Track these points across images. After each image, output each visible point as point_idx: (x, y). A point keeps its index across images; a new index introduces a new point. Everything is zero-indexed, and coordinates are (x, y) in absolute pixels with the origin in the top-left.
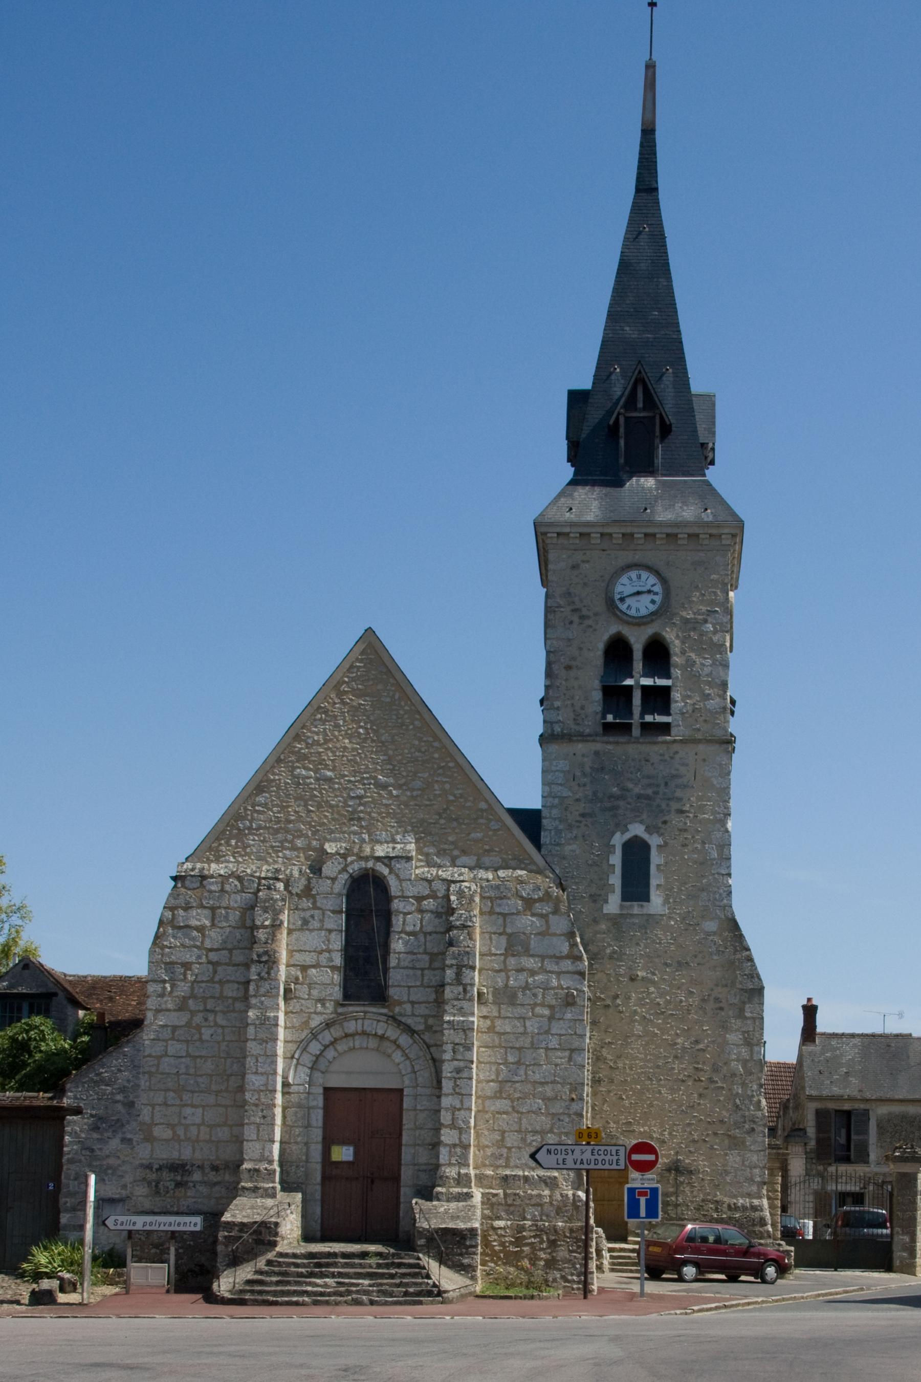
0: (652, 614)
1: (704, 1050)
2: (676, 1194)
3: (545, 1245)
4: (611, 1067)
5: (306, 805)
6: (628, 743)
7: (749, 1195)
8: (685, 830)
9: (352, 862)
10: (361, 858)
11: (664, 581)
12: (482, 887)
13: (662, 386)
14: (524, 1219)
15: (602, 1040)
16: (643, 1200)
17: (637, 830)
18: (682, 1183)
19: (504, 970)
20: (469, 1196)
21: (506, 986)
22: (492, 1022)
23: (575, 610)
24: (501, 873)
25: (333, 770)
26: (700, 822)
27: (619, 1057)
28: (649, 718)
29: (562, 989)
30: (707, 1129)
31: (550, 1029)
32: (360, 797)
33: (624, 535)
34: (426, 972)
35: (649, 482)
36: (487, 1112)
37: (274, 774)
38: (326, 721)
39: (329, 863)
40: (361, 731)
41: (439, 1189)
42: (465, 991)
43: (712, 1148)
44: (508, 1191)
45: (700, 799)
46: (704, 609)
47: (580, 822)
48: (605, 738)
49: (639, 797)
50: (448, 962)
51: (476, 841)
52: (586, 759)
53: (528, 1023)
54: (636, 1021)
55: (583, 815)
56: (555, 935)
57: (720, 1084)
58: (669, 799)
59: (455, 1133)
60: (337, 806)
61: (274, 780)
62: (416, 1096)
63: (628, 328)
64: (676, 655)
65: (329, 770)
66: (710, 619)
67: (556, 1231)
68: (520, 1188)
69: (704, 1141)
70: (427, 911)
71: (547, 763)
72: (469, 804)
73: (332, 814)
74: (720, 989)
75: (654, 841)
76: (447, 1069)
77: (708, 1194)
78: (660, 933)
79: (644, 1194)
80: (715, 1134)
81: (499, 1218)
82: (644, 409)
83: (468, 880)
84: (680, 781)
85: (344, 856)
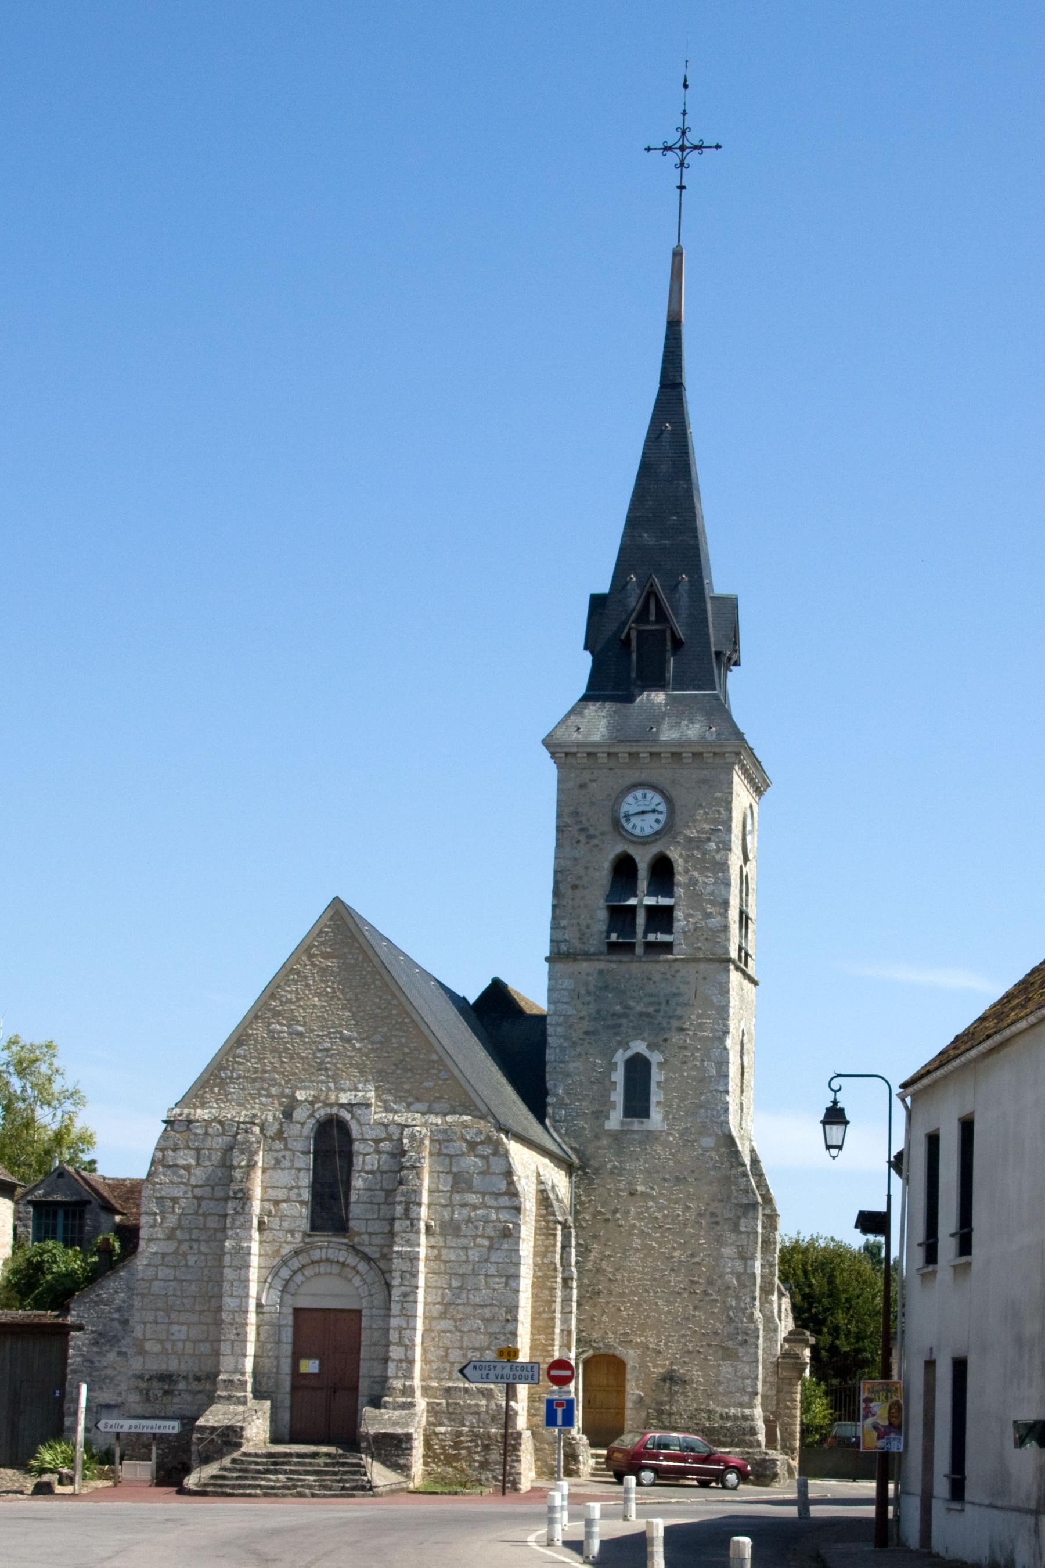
0: (656, 833)
1: (699, 1264)
2: (670, 1403)
3: (479, 1449)
4: (610, 1279)
5: (280, 1057)
6: (631, 962)
7: (741, 1405)
8: (685, 1048)
9: (319, 1109)
10: (326, 1105)
11: (669, 800)
12: (431, 1131)
13: (677, 595)
14: (464, 1425)
15: (601, 1253)
16: (560, 1411)
17: (639, 1047)
18: (676, 1392)
19: (450, 1205)
20: (411, 1405)
21: (452, 1219)
22: (439, 1251)
23: (582, 830)
24: (449, 1118)
25: (304, 1025)
26: (700, 1039)
27: (617, 1270)
28: (651, 937)
29: (500, 1222)
30: (701, 1341)
31: (489, 1258)
32: (327, 1050)
33: (630, 754)
34: (382, 1206)
35: (659, 697)
36: (433, 1331)
37: (252, 1029)
38: (298, 981)
39: (299, 1110)
40: (329, 990)
41: (387, 1399)
42: (412, 1224)
43: (706, 1359)
44: (450, 1401)
45: (699, 1016)
46: (707, 827)
47: (584, 1040)
48: (609, 957)
49: (641, 1015)
50: (398, 1199)
51: (429, 1089)
52: (590, 978)
53: (470, 1253)
54: (635, 1234)
55: (586, 1033)
56: (494, 1174)
57: (714, 1297)
58: (670, 1017)
59: (401, 1350)
60: (307, 1058)
61: (253, 1034)
62: (372, 1316)
63: (646, 535)
64: (680, 873)
65: (300, 1025)
66: (713, 837)
67: (489, 1437)
68: (460, 1398)
69: (699, 1352)
70: (383, 1152)
71: (553, 982)
72: (422, 1056)
73: (303, 1064)
74: (716, 1204)
75: (655, 1058)
76: (396, 1293)
77: (702, 1403)
78: (659, 1148)
79: (561, 1405)
80: (709, 1345)
81: (441, 1425)
82: (657, 621)
83: (420, 1124)
84: (681, 999)
85: (312, 1103)
